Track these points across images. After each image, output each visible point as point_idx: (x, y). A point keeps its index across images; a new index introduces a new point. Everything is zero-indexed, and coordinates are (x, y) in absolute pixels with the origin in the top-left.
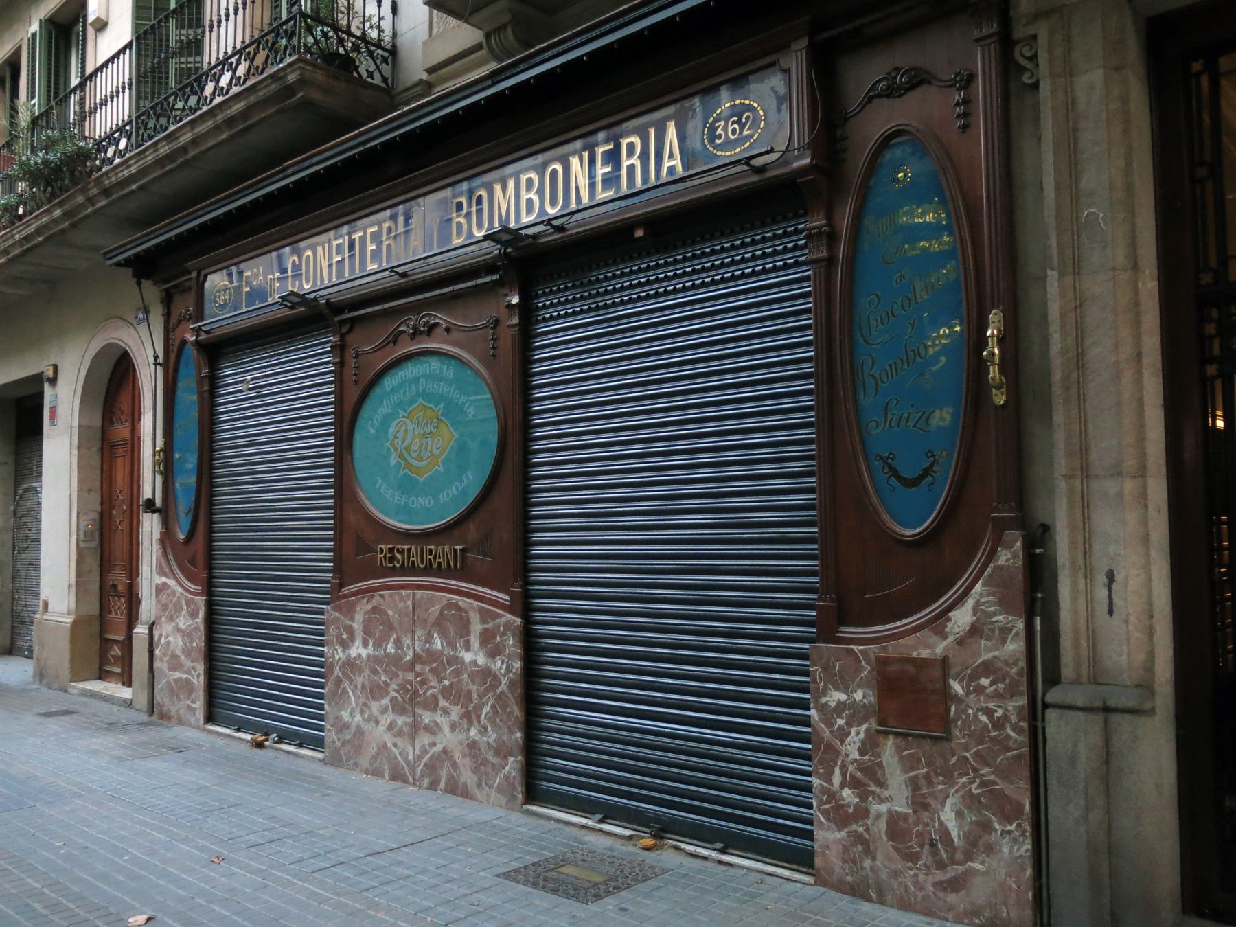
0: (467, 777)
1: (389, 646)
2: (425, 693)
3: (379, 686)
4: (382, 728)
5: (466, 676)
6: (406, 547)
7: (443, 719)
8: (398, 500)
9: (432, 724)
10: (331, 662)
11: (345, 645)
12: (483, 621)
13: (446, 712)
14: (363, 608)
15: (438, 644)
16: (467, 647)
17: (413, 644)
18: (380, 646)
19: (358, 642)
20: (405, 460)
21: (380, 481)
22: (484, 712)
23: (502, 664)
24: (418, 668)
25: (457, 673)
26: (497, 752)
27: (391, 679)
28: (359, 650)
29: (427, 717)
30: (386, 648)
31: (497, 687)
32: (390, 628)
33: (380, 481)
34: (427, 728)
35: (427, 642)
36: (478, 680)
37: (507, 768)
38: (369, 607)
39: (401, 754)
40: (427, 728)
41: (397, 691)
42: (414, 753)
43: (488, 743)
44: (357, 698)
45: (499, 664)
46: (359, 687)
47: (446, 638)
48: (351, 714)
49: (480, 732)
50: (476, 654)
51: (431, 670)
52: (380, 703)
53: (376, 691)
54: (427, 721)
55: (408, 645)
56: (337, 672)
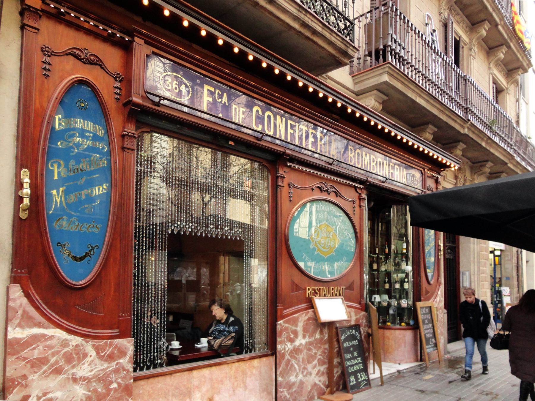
1: (317, 335)
10: (283, 353)
11: (292, 341)
12: (356, 315)
18: (312, 336)
19: (300, 336)
20: (318, 247)
21: (305, 255)
27: (318, 351)
28: (300, 341)
30: (315, 336)
33: (305, 255)
44: (299, 366)
46: (301, 360)
52: (312, 364)
56: (287, 357)
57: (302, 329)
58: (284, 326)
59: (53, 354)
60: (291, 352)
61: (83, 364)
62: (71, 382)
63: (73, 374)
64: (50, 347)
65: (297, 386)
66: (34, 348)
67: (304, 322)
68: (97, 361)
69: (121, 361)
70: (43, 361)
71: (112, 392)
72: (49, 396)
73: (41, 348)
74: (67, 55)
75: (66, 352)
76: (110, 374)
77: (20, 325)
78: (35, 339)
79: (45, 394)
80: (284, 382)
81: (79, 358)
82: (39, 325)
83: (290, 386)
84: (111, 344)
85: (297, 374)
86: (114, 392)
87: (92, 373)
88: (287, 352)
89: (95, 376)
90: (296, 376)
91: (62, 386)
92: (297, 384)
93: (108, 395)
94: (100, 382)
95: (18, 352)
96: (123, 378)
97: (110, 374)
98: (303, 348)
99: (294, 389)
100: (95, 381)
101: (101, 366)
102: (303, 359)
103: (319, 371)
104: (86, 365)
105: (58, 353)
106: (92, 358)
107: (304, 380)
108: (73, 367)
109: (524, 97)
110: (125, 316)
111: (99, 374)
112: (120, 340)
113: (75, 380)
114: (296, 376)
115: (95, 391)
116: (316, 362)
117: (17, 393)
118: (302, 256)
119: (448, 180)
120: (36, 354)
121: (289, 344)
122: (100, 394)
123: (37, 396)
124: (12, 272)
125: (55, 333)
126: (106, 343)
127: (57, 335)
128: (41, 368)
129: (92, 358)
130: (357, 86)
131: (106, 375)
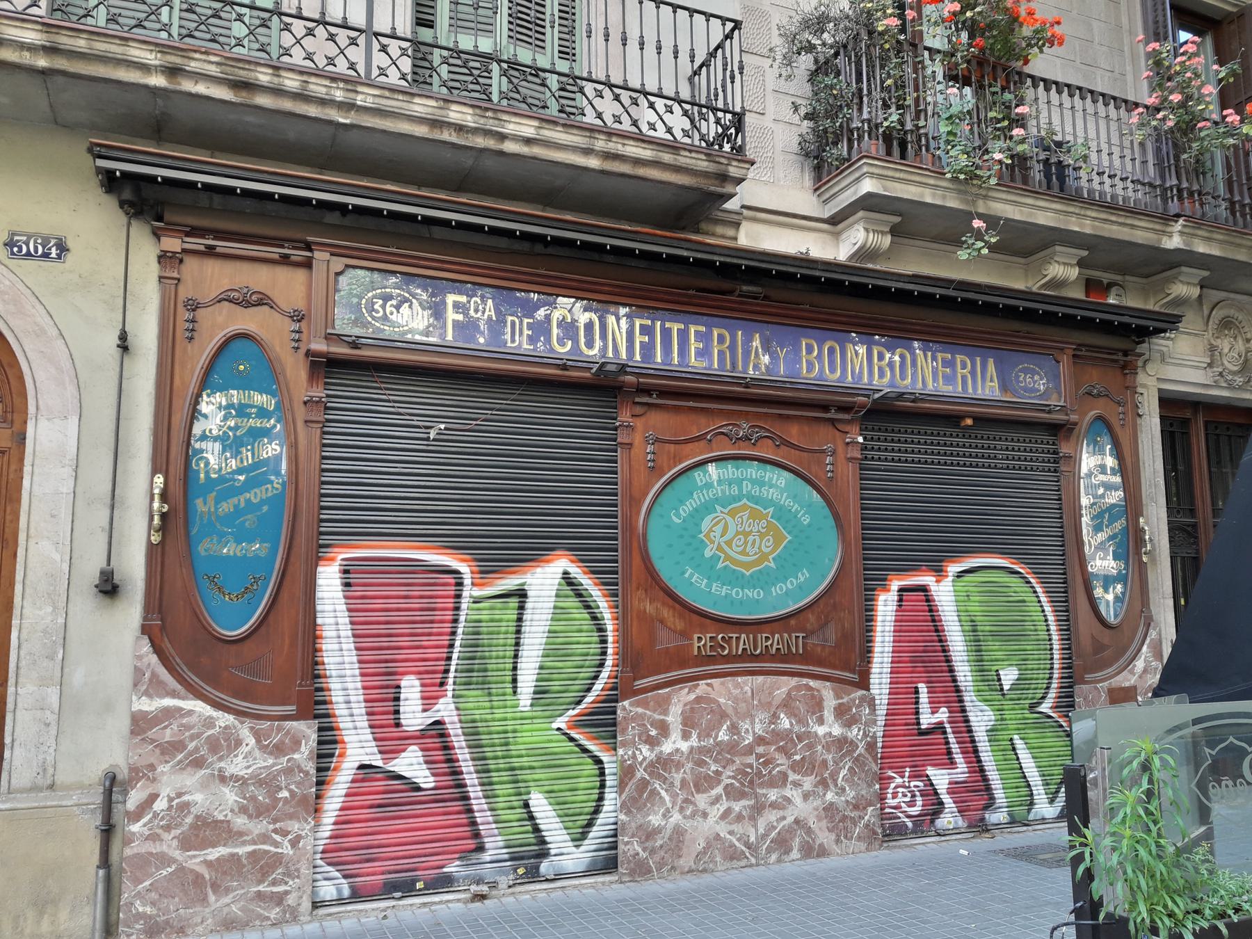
0: (824, 837)
1: (721, 734)
2: (770, 772)
3: (707, 777)
4: (711, 820)
5: (820, 747)
6: (735, 635)
7: (794, 792)
8: (716, 590)
9: (780, 800)
12: (838, 696)
13: (797, 784)
14: (681, 699)
15: (785, 723)
16: (821, 721)
17: (753, 728)
18: (709, 735)
19: (675, 735)
20: (725, 553)
22: (841, 776)
23: (859, 731)
24: (760, 750)
25: (810, 746)
26: (856, 807)
27: (724, 767)
28: (674, 744)
29: (773, 795)
30: (717, 736)
31: (855, 751)
32: (723, 715)
33: (690, 571)
34: (774, 805)
35: (771, 723)
36: (833, 749)
37: (866, 818)
38: (692, 696)
39: (739, 840)
40: (774, 805)
41: (733, 778)
42: (757, 833)
43: (847, 801)
44: (674, 796)
45: (855, 731)
46: (677, 783)
47: (795, 716)
48: (664, 816)
49: (837, 794)
50: (830, 726)
51: (779, 749)
52: (709, 794)
53: (703, 783)
54: (773, 798)
55: (747, 730)
56: (641, 773)
57: (679, 720)
58: (631, 711)
59: (192, 738)
60: (651, 764)
61: (236, 756)
62: (217, 781)
63: (220, 770)
64: (188, 727)
65: (667, 836)
66: (166, 727)
67: (685, 705)
68: (257, 753)
69: (296, 756)
70: (178, 746)
71: (280, 805)
72: (186, 798)
73: (175, 727)
74: (219, 302)
75: (209, 736)
76: (278, 775)
77: (146, 693)
78: (168, 713)
79: (179, 795)
80: (633, 825)
81: (229, 746)
82: (174, 694)
83: (649, 834)
84: (279, 729)
85: (668, 810)
86: (284, 805)
87: (249, 771)
88: (641, 764)
89: (252, 776)
90: (665, 816)
91: (204, 785)
92: (669, 832)
93: (274, 808)
94: (261, 785)
95: (145, 732)
96: (298, 784)
97: (278, 775)
98: (683, 760)
99: (659, 843)
100: (253, 784)
101: (265, 762)
102: (684, 782)
103: (728, 812)
104: (241, 757)
105: (198, 736)
106: (249, 747)
107: (687, 825)
108: (221, 759)
109: (99, 170)
110: (306, 686)
111: (259, 775)
112: (295, 723)
113: (223, 779)
114: (665, 816)
115: (253, 798)
116: (719, 790)
117: (143, 787)
118: (684, 573)
119: (1173, 361)
120: (168, 736)
121: (645, 749)
122: (262, 804)
123: (168, 796)
124: (145, 619)
125: (195, 706)
126: (272, 726)
127: (197, 709)
128: (175, 757)
129: (249, 747)
130: (827, 207)
131: (271, 776)
